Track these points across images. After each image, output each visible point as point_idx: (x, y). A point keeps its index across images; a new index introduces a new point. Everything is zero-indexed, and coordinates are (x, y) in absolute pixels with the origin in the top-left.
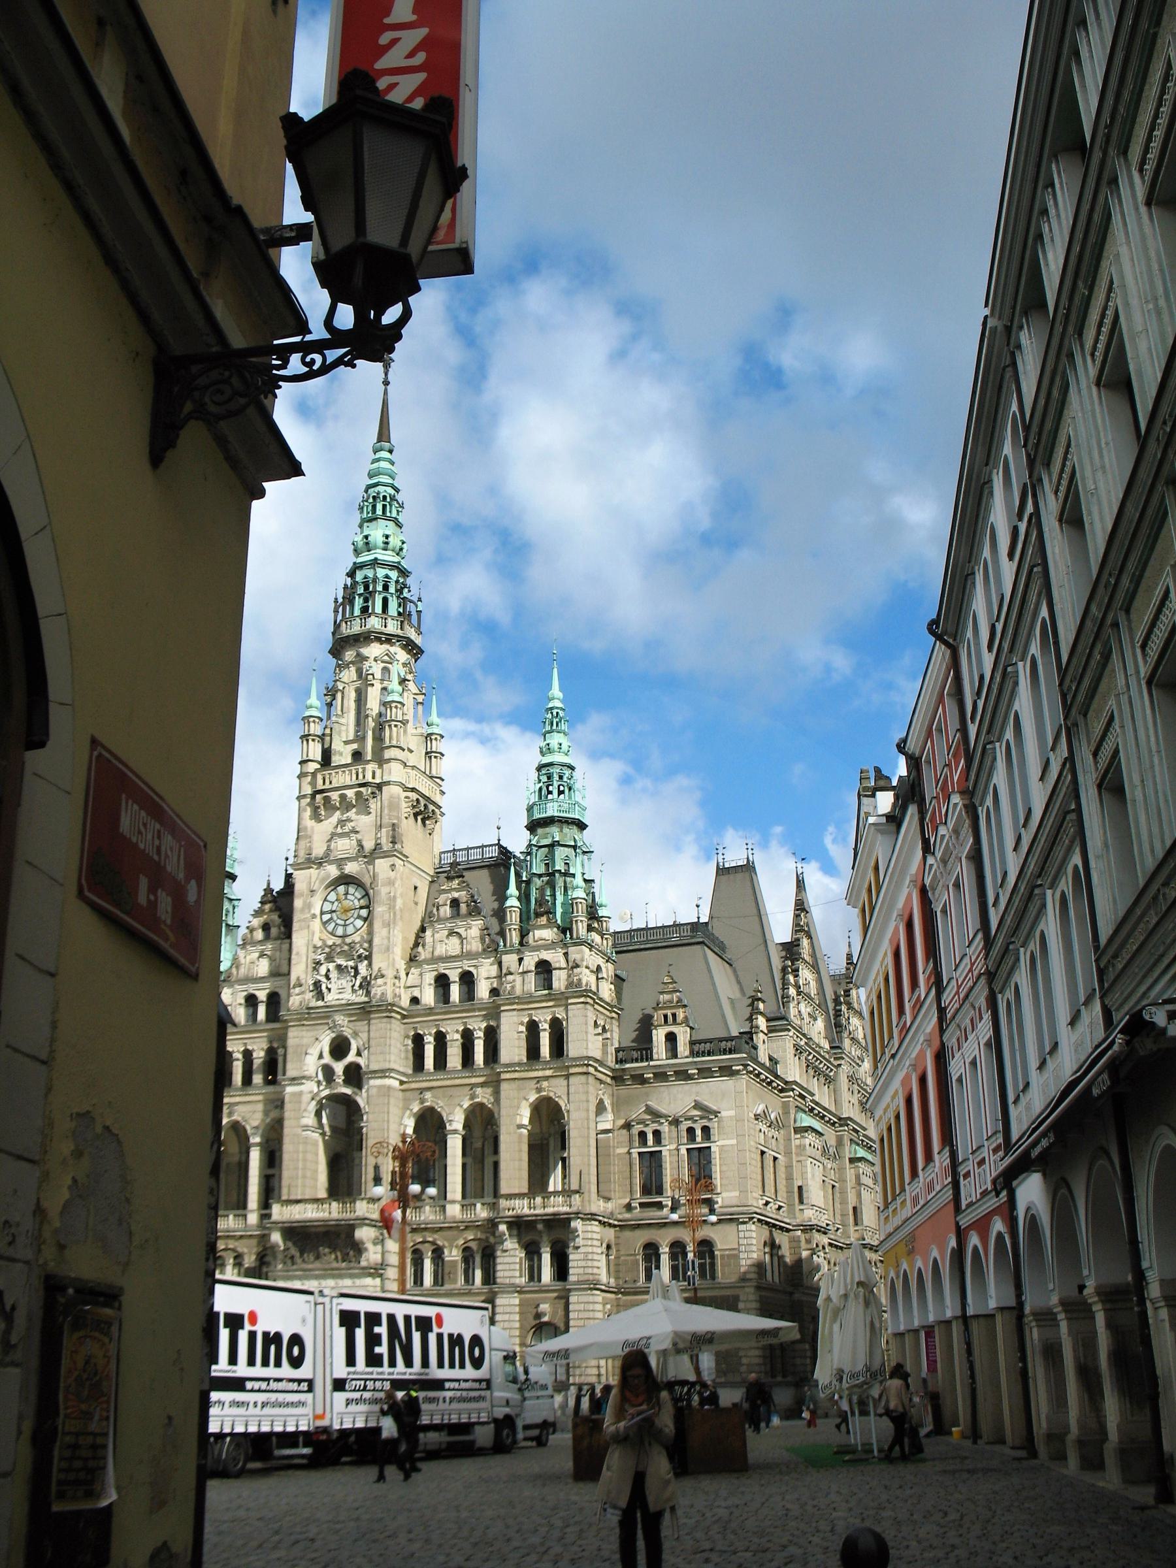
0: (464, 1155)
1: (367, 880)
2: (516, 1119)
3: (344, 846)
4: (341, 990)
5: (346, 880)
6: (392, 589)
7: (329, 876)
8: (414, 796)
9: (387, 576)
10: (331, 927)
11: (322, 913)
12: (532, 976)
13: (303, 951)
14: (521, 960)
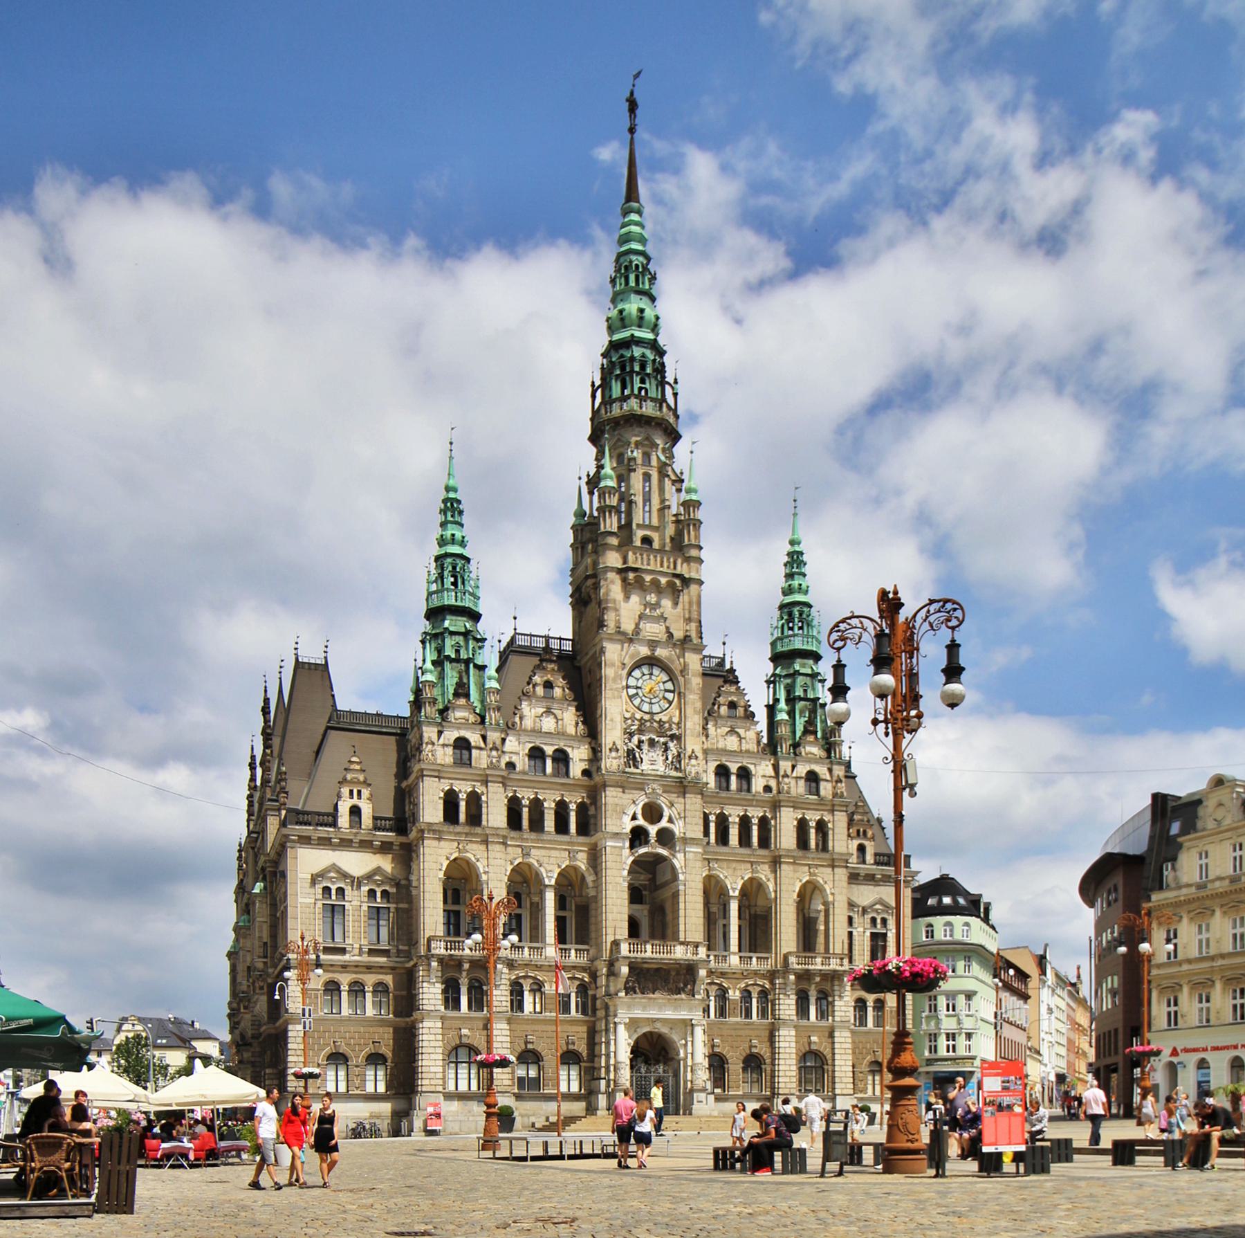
0: (740, 918)
1: (676, 667)
3: (653, 630)
4: (653, 762)
5: (651, 662)
10: (637, 702)
12: (802, 783)
13: (618, 719)
14: (793, 767)
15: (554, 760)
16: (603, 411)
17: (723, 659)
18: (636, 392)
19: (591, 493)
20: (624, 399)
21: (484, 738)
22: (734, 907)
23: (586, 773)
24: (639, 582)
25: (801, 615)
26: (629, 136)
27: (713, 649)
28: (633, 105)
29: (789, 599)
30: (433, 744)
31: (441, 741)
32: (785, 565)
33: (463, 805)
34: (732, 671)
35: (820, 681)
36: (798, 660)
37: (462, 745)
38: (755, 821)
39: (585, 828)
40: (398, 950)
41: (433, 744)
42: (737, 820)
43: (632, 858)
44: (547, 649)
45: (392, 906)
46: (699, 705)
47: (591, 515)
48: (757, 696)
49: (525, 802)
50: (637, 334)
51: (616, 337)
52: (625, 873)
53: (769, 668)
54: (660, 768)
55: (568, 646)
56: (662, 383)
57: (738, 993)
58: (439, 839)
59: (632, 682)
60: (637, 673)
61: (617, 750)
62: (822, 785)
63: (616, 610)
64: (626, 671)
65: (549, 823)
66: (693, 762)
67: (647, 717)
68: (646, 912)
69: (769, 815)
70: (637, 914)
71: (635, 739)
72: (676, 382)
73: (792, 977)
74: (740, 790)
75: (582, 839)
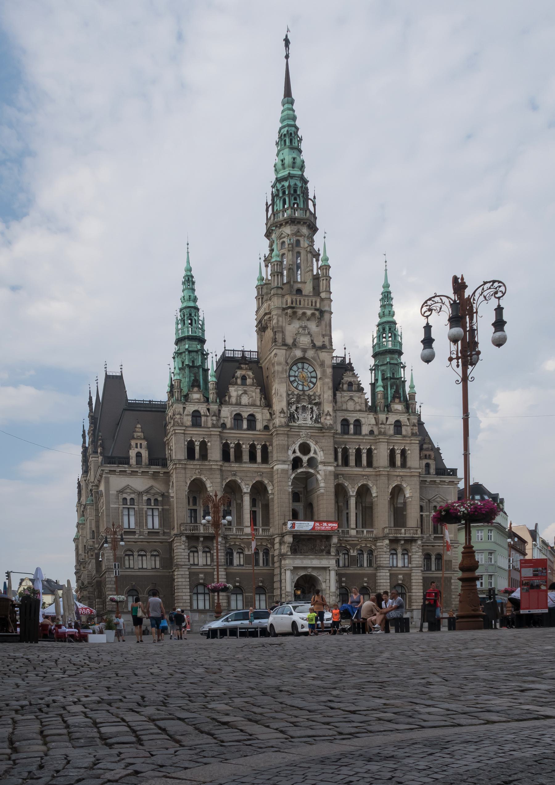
0: (356, 509)
7: (295, 356)
10: (295, 385)
11: (289, 376)
13: (284, 395)
14: (387, 418)
15: (248, 420)
16: (272, 218)
17: (344, 358)
18: (292, 205)
19: (267, 266)
20: (284, 210)
21: (208, 410)
22: (353, 501)
23: (266, 428)
25: (390, 329)
26: (286, 60)
27: (338, 352)
28: (287, 42)
29: (385, 319)
30: (181, 415)
31: (186, 412)
32: (380, 300)
33: (197, 449)
34: (350, 364)
35: (402, 367)
36: (390, 355)
38: (365, 451)
39: (265, 459)
40: (164, 532)
41: (181, 415)
42: (354, 451)
43: (293, 475)
44: (243, 357)
45: (160, 508)
46: (331, 385)
47: (267, 279)
48: (365, 378)
49: (232, 445)
50: (292, 172)
51: (279, 176)
52: (290, 483)
53: (372, 362)
54: (309, 422)
55: (254, 356)
56: (306, 199)
57: (355, 552)
58: (185, 468)
59: (292, 373)
60: (295, 368)
61: (284, 413)
62: (404, 429)
63: (283, 332)
64: (288, 368)
65: (246, 457)
66: (328, 417)
67: (301, 393)
68: (302, 507)
70: (296, 508)
71: (294, 407)
72: (314, 198)
73: (387, 542)
75: (264, 466)
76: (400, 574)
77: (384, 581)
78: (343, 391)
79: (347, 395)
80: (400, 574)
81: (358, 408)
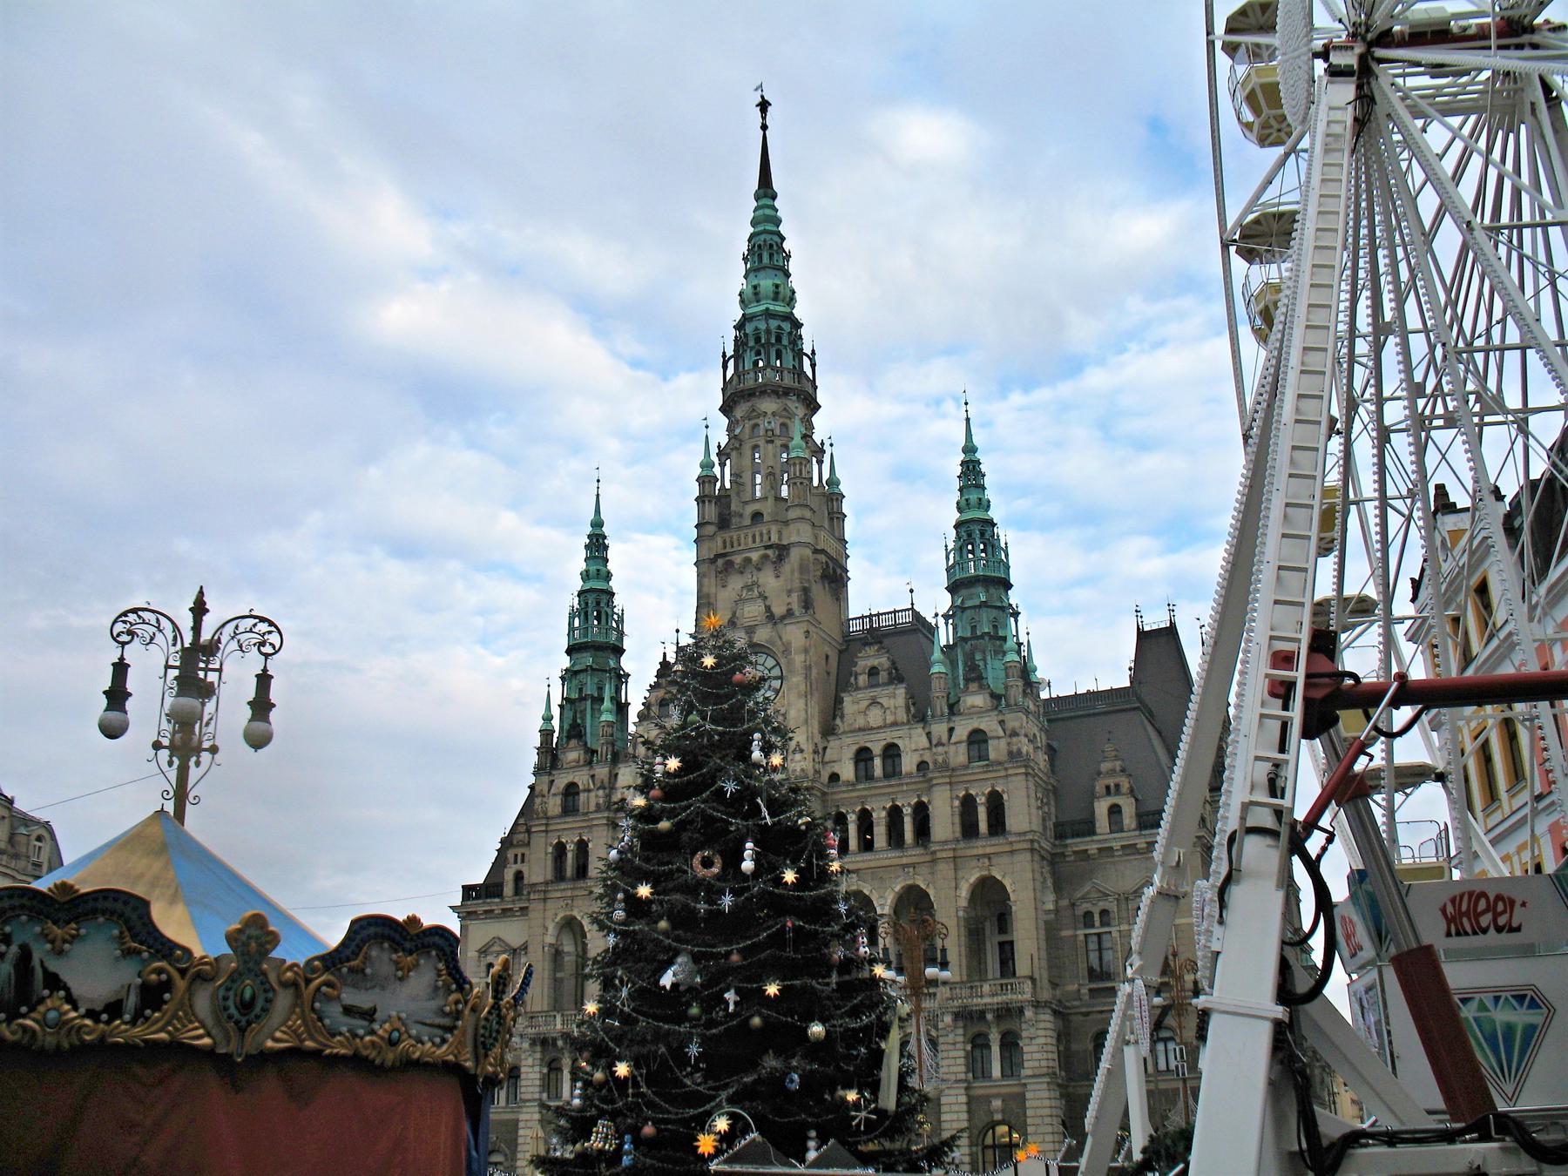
2: (951, 903)
6: (785, 341)
8: (823, 558)
9: (779, 327)
12: (963, 748)
24: (730, 564)
37: (571, 791)
42: (884, 814)
66: (798, 756)
69: (925, 799)
74: (887, 776)
76: (997, 1096)
77: (955, 1117)
78: (858, 689)
79: (863, 697)
80: (997, 1096)
81: (890, 719)
